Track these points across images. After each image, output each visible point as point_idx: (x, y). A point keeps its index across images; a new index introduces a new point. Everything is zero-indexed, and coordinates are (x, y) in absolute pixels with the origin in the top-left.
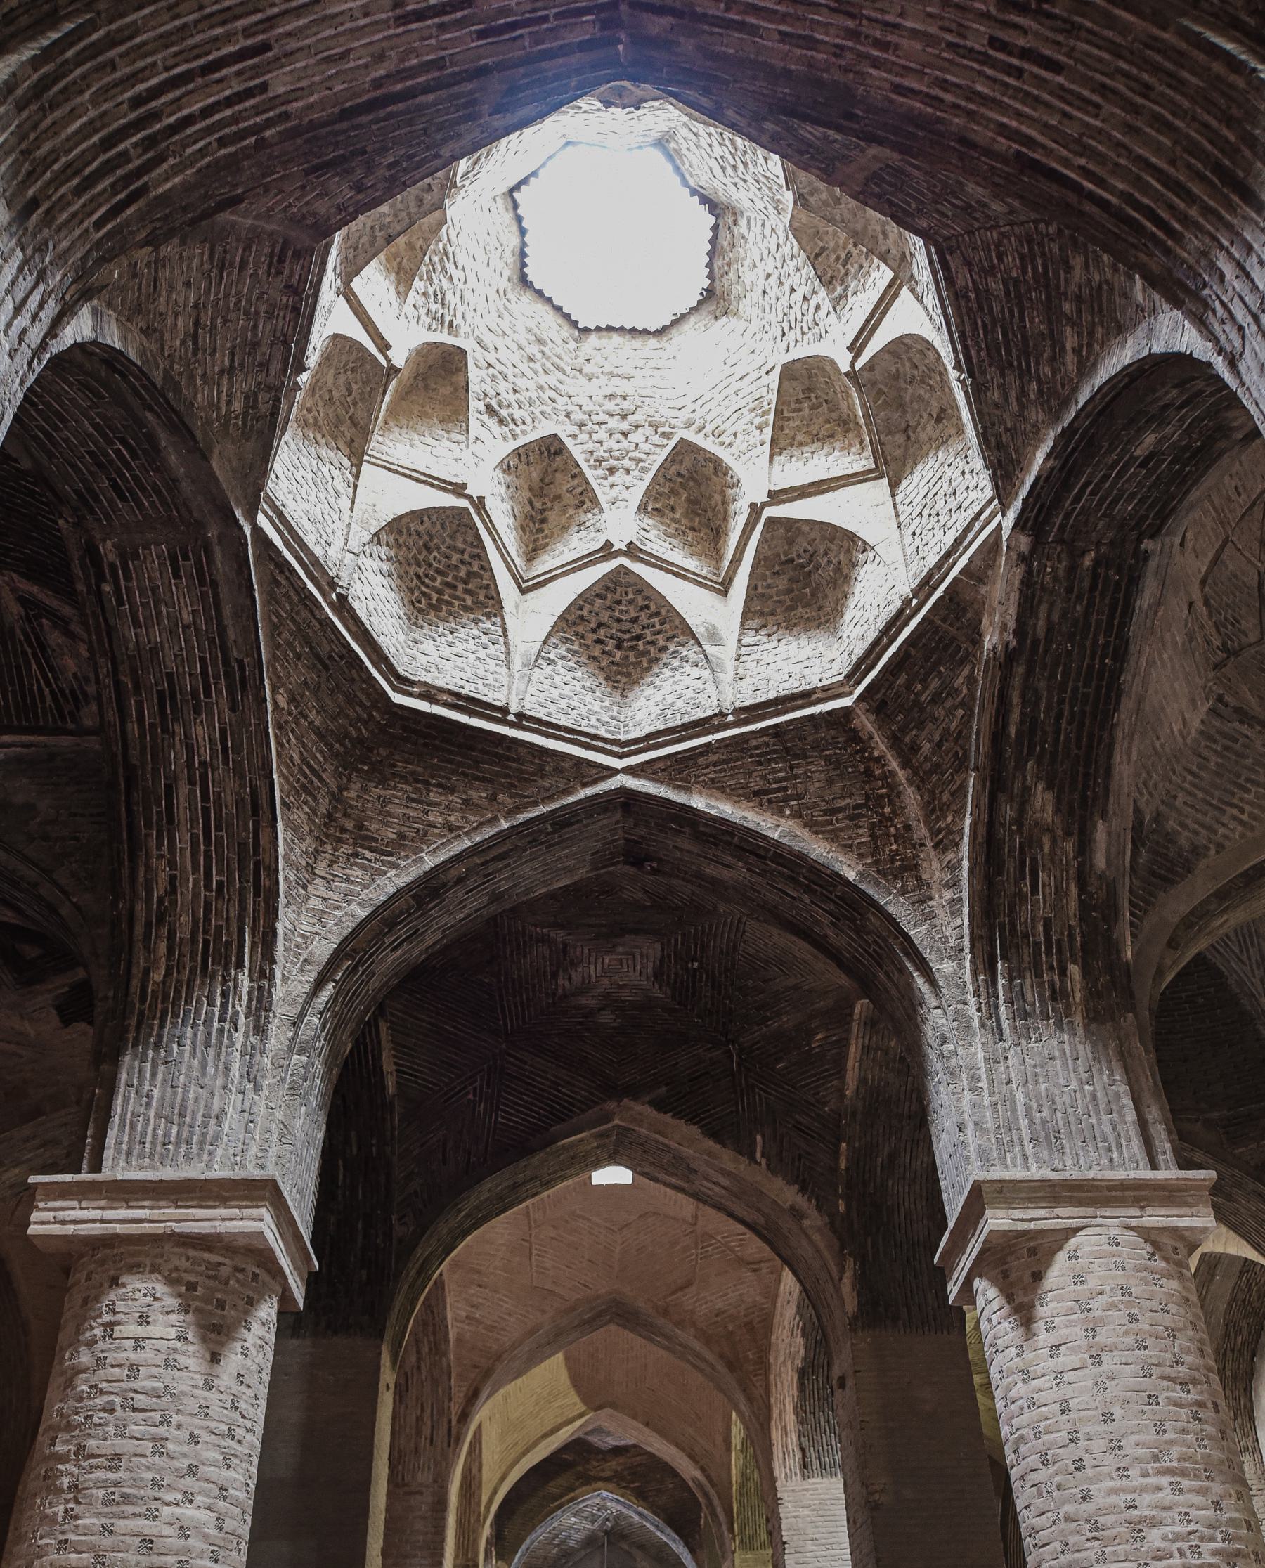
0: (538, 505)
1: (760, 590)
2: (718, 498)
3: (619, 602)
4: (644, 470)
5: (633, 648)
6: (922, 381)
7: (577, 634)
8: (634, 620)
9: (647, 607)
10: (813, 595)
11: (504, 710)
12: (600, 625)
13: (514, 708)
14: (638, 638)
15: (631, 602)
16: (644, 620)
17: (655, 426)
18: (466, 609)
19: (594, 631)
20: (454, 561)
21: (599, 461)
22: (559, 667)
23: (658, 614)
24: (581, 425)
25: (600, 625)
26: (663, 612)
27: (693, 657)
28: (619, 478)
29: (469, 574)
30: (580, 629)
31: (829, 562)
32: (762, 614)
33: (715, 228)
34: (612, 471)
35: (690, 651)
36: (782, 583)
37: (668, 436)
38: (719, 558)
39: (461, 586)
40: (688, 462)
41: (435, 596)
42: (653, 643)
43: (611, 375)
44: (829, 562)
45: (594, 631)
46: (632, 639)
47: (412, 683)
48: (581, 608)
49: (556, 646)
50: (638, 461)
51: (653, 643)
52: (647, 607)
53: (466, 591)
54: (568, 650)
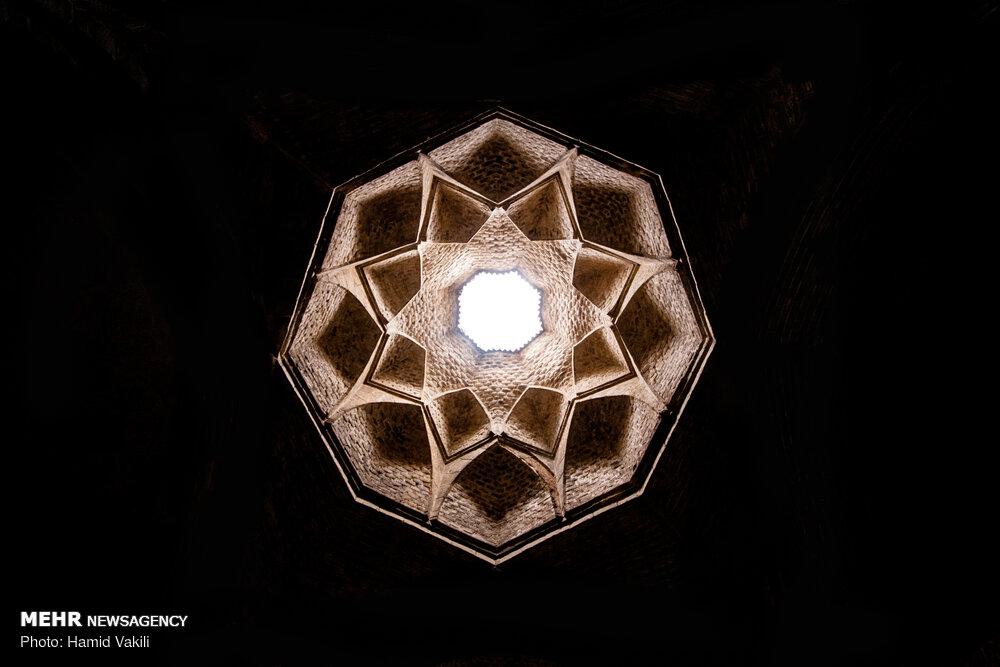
0: (544, 206)
1: (413, 204)
2: (445, 218)
3: (500, 182)
4: (486, 227)
5: (491, 157)
6: (348, 341)
7: (527, 168)
8: (490, 173)
9: (482, 182)
10: (380, 210)
11: (580, 152)
12: (512, 170)
13: (574, 151)
14: (487, 164)
15: (493, 182)
16: (484, 175)
17: (480, 243)
18: (596, 190)
19: (516, 168)
20: (596, 212)
21: (509, 229)
22: (540, 155)
23: (477, 178)
24: (518, 241)
25: (512, 170)
26: (472, 181)
27: (451, 165)
28: (498, 225)
29: (589, 204)
30: (525, 170)
31: (375, 231)
32: (410, 193)
33: (457, 323)
34: (503, 227)
35: (451, 167)
36: (401, 210)
37: (473, 241)
38: (442, 192)
39: (596, 199)
40: (462, 232)
41: (613, 198)
42: (478, 163)
43: (503, 258)
44: (375, 231)
45: (516, 168)
46: (491, 162)
47: (642, 177)
48: (523, 180)
49: (541, 165)
50: (489, 231)
51: (478, 163)
52: (482, 182)
53: (593, 197)
54: (532, 161)
